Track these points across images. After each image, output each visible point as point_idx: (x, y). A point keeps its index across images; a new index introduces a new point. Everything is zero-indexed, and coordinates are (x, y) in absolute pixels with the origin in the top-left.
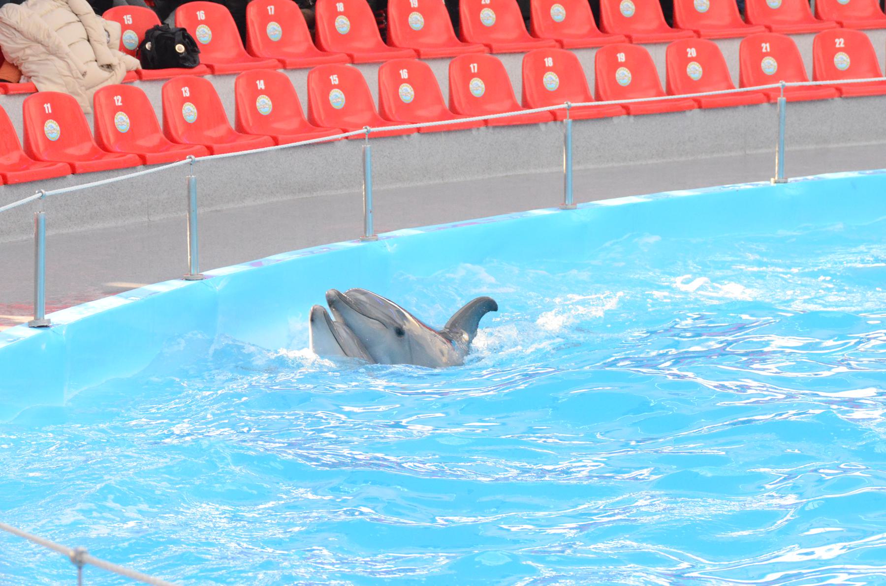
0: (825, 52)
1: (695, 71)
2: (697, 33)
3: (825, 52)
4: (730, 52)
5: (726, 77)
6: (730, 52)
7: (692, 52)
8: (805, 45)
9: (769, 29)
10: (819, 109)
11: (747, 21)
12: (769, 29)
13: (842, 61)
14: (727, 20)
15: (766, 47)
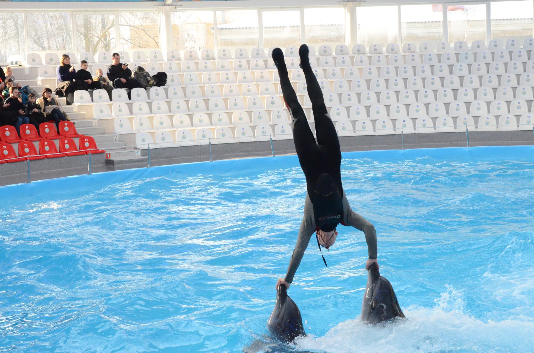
0: (42, 146)
1: (6, 152)
2: (7, 142)
3: (42, 146)
4: (16, 147)
5: (14, 154)
6: (16, 147)
7: (5, 147)
8: (36, 144)
9: (27, 140)
10: (41, 162)
11: (21, 138)
12: (27, 140)
13: (47, 148)
14: (15, 138)
15: (26, 145)
